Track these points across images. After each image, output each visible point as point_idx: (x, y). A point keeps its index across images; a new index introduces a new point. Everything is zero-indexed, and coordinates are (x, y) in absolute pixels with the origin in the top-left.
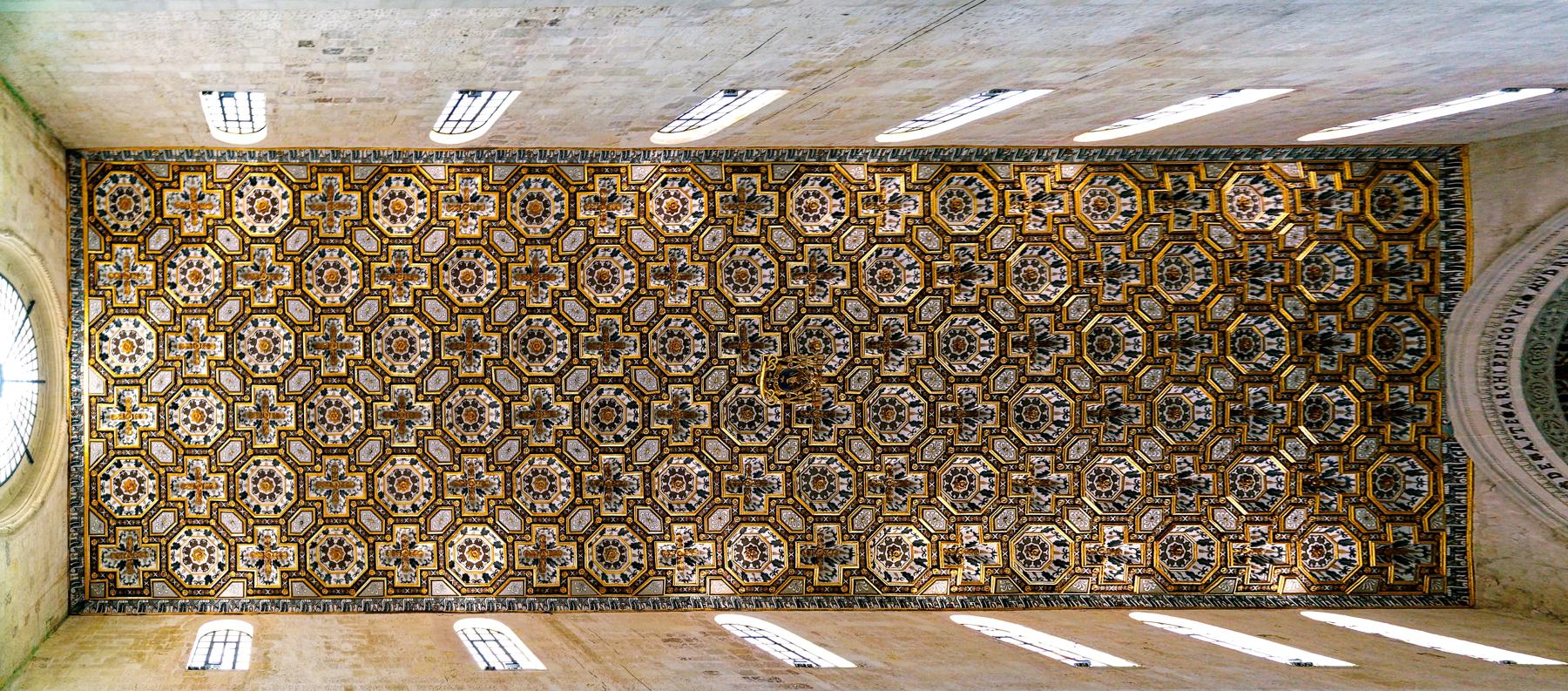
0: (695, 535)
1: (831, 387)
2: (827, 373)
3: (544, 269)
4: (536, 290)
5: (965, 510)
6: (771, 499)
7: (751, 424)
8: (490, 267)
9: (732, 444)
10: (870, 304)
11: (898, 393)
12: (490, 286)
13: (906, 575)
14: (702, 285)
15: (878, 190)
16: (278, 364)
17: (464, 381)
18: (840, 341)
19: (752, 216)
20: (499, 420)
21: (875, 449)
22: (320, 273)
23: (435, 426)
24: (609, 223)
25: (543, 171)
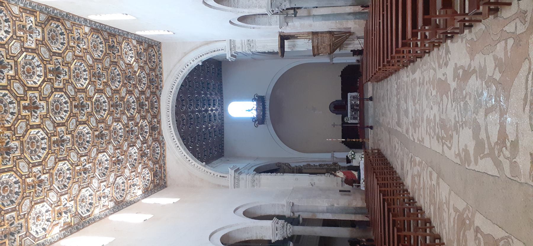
1: (8, 133)
2: (7, 125)
5: (63, 189)
10: (24, 85)
11: (36, 134)
15: (24, 22)
18: (11, 106)
21: (29, 165)
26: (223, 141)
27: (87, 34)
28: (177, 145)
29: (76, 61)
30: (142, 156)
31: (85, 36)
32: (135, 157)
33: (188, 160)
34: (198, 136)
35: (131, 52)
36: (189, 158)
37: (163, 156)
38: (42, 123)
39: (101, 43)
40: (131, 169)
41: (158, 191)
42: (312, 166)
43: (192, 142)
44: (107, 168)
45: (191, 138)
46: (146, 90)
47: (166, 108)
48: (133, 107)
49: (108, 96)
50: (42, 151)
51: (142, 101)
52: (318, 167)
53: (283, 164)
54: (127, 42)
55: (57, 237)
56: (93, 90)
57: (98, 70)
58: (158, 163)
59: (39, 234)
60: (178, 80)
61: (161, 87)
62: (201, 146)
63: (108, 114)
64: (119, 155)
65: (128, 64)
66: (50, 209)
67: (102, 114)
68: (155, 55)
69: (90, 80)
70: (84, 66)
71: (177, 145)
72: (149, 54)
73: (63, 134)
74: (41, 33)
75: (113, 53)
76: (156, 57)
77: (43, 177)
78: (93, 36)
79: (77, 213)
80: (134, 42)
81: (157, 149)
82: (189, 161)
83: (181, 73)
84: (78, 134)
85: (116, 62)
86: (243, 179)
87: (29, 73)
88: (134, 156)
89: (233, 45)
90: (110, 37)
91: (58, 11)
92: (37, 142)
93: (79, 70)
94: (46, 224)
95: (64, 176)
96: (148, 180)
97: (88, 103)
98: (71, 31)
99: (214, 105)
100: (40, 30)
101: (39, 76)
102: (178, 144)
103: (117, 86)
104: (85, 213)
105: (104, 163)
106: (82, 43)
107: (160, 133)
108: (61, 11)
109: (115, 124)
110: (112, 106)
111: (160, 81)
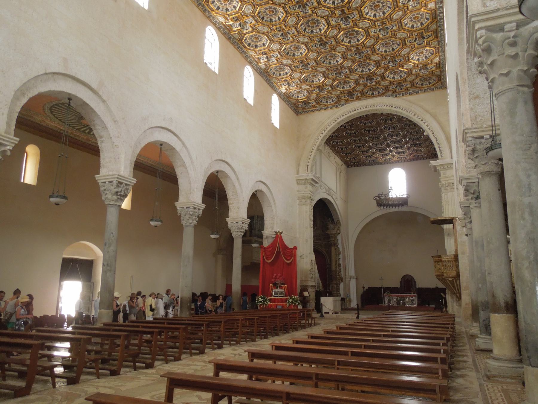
26: (363, 166)
28: (337, 120)
30: (318, 87)
32: (315, 81)
33: (323, 132)
34: (359, 140)
35: (424, 58)
36: (324, 133)
37: (326, 108)
39: (422, 24)
40: (302, 78)
41: (290, 108)
42: (339, 256)
43: (351, 134)
44: (294, 55)
45: (355, 133)
46: (386, 80)
47: (374, 104)
48: (364, 70)
49: (365, 43)
51: (374, 78)
52: (338, 263)
53: (339, 227)
54: (433, 52)
55: (216, 21)
56: (366, 26)
57: (390, 27)
58: (317, 103)
59: (213, 4)
60: (405, 112)
61: (396, 96)
62: (350, 144)
63: (346, 46)
64: (311, 65)
65: (408, 56)
67: (345, 40)
68: (431, 85)
69: (375, 21)
70: (388, 11)
71: (337, 120)
72: (429, 77)
73: (310, 5)
75: (416, 39)
76: (428, 85)
78: (427, 13)
79: (243, 35)
80: (437, 60)
81: (331, 101)
82: (322, 133)
83: (413, 114)
84: (316, 21)
85: (406, 44)
86: (306, 188)
88: (316, 80)
89: (446, 167)
90: (432, 32)
94: (223, 8)
95: (271, 15)
96: (298, 97)
99: (399, 153)
102: (338, 121)
103: (381, 50)
104: (246, 43)
105: (298, 52)
106: (414, 3)
107: (347, 101)
109: (340, 55)
110: (357, 48)
111: (402, 94)
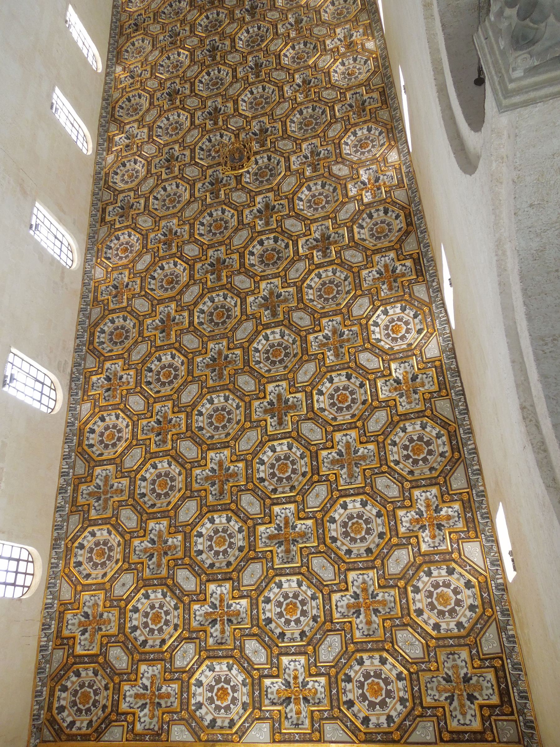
0: (356, 181)
1: (242, 136)
3: (162, 321)
4: (177, 324)
6: (321, 145)
7: (271, 170)
8: (159, 360)
9: (285, 176)
12: (173, 357)
13: (365, 63)
14: (175, 221)
16: (236, 528)
17: (246, 362)
19: (133, 204)
20: (277, 330)
22: (159, 496)
23: (285, 380)
24: (132, 286)
25: (92, 335)
27: (125, 68)
29: (157, 74)
31: (127, 69)
38: (231, 98)
39: (133, 44)
50: (267, 90)
54: (128, 5)
66: (340, 60)
74: (131, 125)
77: (299, 81)
78: (126, 59)
87: (177, 128)
91: (103, 111)
92: (255, 99)
93: (169, 66)
97: (208, 43)
98: (124, 89)
100: (128, 127)
101: (179, 116)
108: (102, 108)
